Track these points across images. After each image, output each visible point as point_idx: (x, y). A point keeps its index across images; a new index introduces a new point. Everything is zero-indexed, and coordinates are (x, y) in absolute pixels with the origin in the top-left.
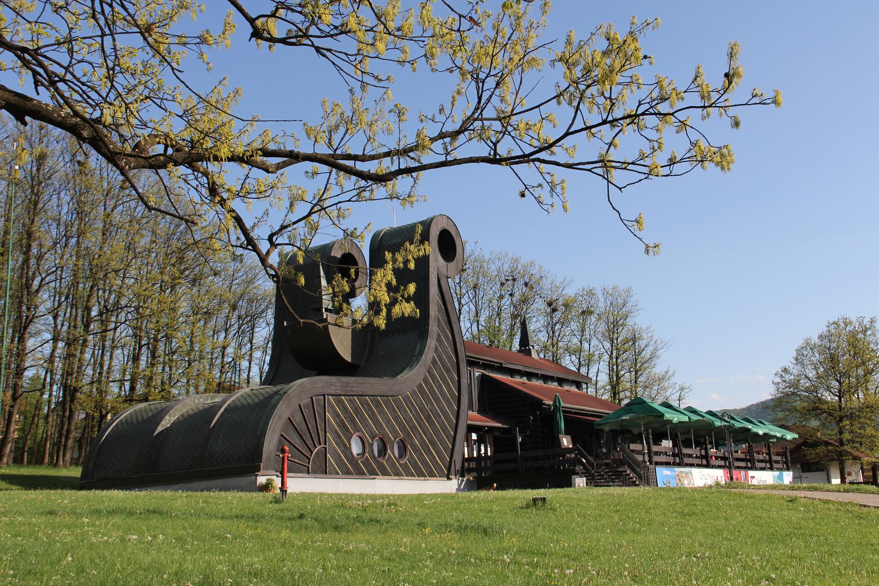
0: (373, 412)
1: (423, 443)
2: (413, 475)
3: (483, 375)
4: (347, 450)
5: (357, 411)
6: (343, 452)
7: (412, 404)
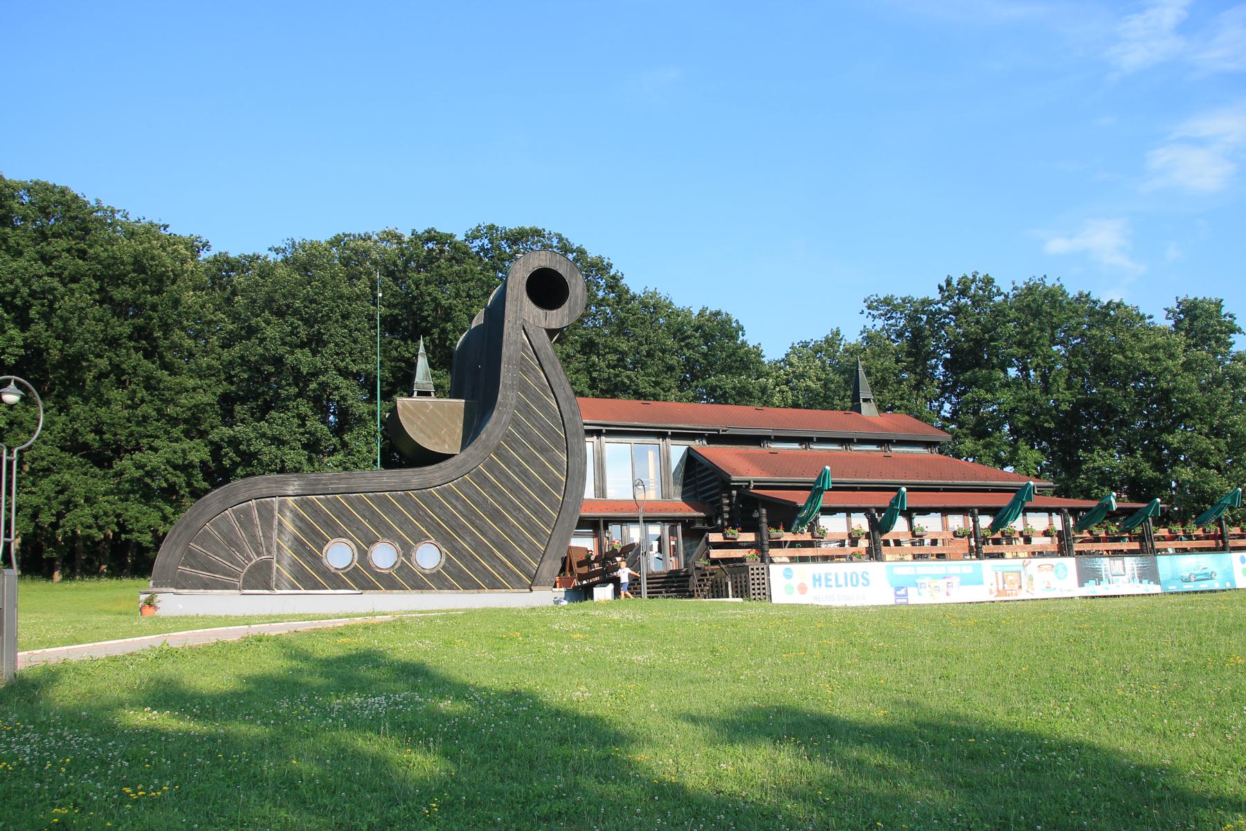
0: (374, 512)
2: (452, 587)
3: (689, 449)
4: (316, 561)
5: (341, 513)
6: (308, 563)
7: (458, 498)
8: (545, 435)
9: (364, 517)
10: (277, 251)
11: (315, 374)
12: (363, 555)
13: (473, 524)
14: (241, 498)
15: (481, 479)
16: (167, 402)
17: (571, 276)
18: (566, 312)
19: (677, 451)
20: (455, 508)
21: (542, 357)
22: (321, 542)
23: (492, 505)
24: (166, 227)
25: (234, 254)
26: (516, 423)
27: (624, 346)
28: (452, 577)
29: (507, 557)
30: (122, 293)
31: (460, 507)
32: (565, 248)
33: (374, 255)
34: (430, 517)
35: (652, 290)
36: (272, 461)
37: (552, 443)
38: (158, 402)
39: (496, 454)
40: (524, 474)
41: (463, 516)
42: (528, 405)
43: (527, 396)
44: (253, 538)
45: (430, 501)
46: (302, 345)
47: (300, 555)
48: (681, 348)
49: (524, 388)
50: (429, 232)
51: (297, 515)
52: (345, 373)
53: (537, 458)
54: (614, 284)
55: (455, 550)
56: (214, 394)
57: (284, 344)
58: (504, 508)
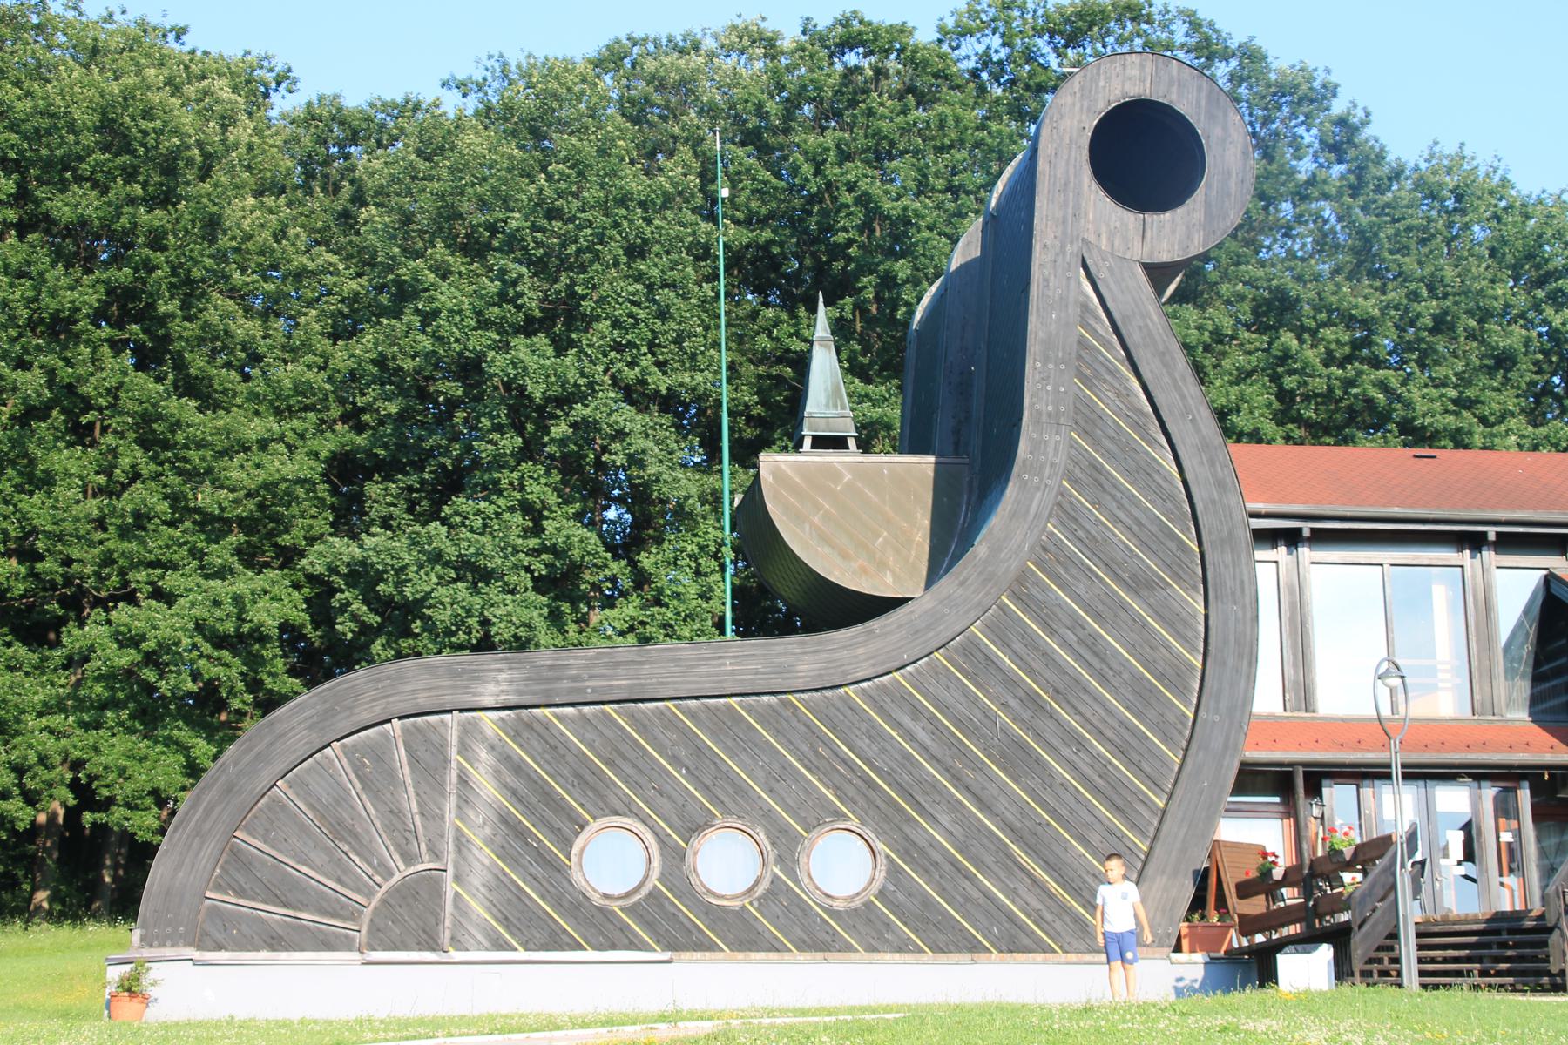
0: (700, 750)
1: (970, 837)
2: (902, 947)
3: (1550, 580)
4: (553, 873)
5: (618, 752)
7: (916, 711)
8: (1143, 544)
9: (675, 760)
10: (463, 87)
11: (565, 400)
12: (674, 858)
13: (956, 779)
14: (366, 717)
15: (976, 661)
16: (195, 476)
17: (1211, 117)
18: (1199, 215)
19: (1515, 585)
20: (910, 737)
21: (1133, 338)
22: (568, 828)
23: (1005, 730)
24: (180, 32)
25: (354, 100)
26: (1066, 513)
27: (1369, 306)
28: (905, 918)
29: (1049, 866)
30: (74, 203)
31: (922, 736)
32: (1208, 48)
33: (710, 93)
34: (845, 762)
35: (1450, 148)
36: (459, 623)
37: (1167, 566)
38: (174, 480)
39: (1016, 597)
40: (1091, 648)
41: (933, 759)
42: (1097, 468)
43: (1096, 444)
44: (395, 815)
45: (844, 720)
46: (529, 328)
47: (514, 861)
48: (1537, 307)
49: (1087, 422)
50: (845, 23)
51: (506, 758)
52: (636, 395)
53: (1124, 607)
54: (1343, 139)
55: (911, 849)
56: (316, 455)
57: (484, 324)
58: (1038, 736)
